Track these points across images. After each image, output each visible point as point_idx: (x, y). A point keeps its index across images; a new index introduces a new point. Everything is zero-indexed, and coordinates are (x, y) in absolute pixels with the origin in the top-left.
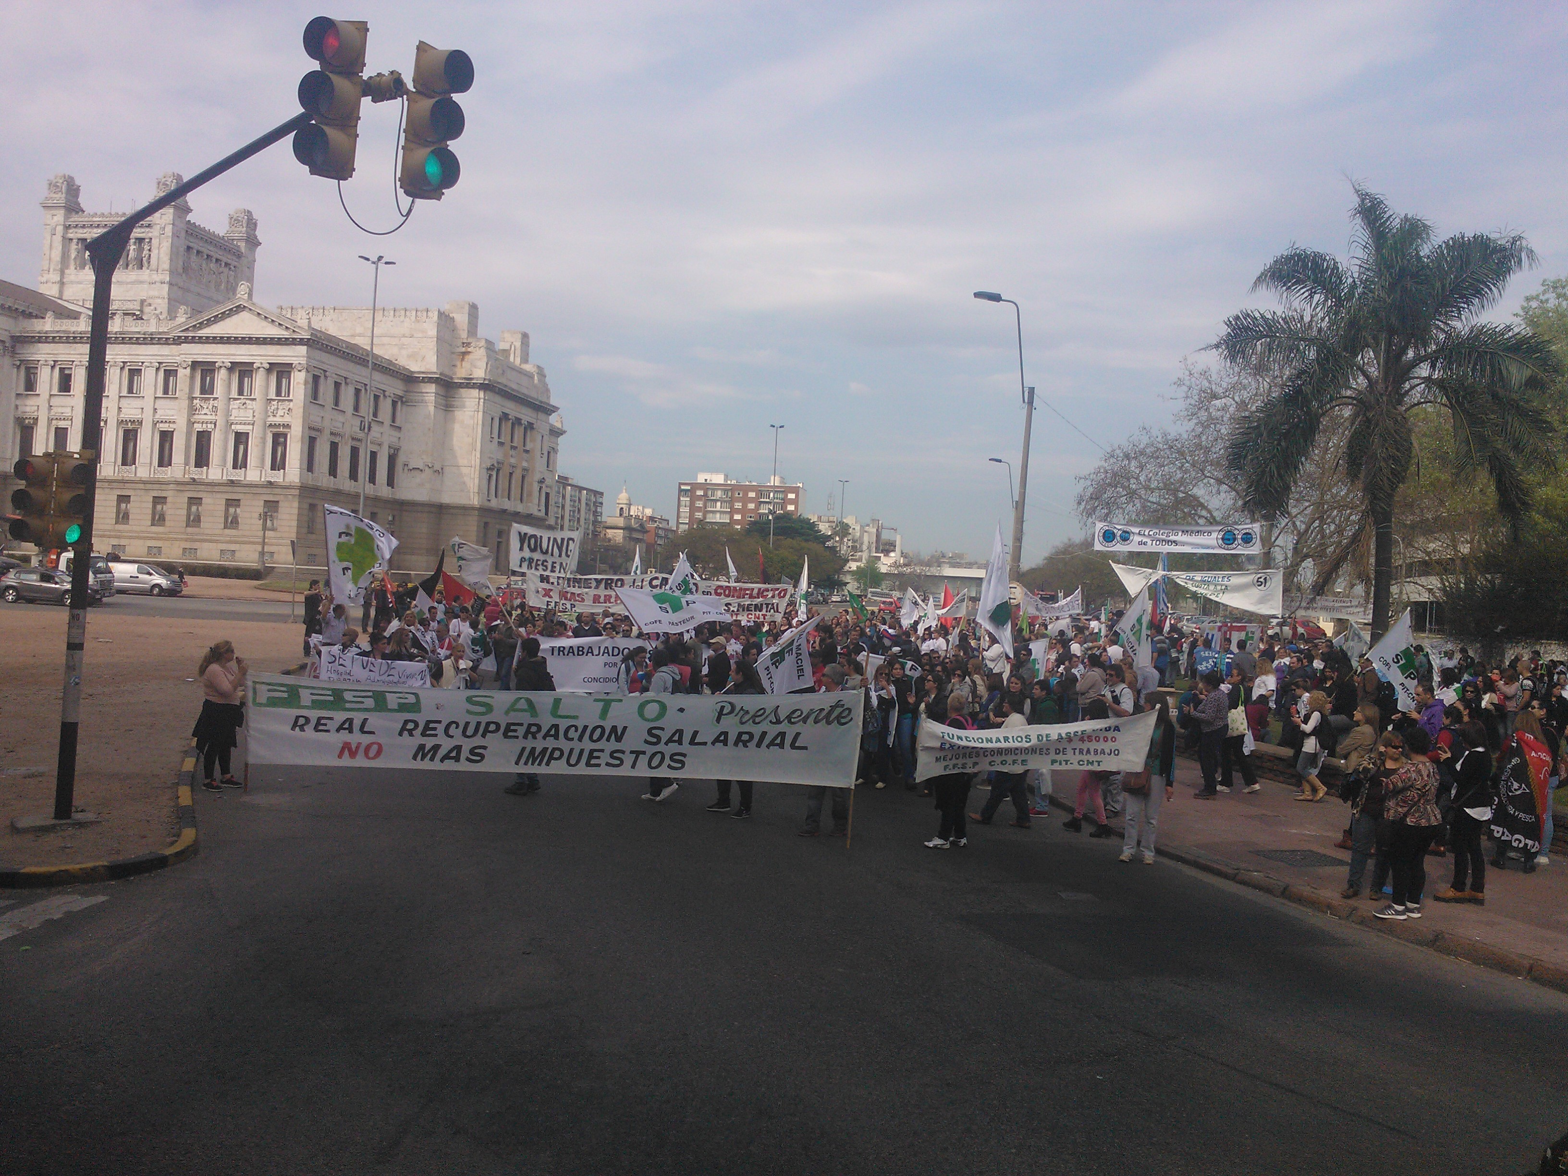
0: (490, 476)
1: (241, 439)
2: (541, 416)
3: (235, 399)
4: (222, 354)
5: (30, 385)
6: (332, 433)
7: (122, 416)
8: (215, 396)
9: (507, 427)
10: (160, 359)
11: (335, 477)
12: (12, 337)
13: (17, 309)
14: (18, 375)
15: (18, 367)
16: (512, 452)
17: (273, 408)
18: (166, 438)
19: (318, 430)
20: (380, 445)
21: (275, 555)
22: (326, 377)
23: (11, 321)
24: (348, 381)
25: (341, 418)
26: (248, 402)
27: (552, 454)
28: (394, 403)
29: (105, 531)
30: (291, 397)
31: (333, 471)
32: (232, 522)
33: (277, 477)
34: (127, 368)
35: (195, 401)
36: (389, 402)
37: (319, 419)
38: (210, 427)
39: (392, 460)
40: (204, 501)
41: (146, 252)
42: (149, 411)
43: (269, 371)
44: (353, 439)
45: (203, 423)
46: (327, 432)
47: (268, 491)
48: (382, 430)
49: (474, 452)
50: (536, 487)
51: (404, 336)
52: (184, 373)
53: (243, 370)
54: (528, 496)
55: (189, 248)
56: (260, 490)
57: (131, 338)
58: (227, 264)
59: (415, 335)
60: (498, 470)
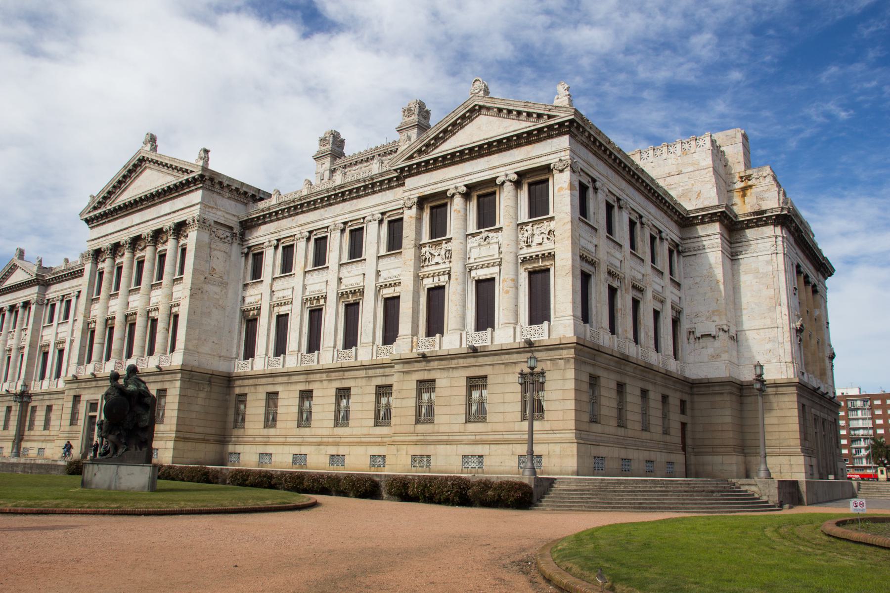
1: (485, 290)
3: (473, 235)
5: (257, 273)
8: (448, 236)
10: (383, 209)
12: (241, 222)
17: (526, 235)
18: (391, 305)
22: (596, 189)
23: (240, 206)
24: (622, 203)
26: (491, 235)
29: (322, 436)
30: (551, 214)
32: (476, 413)
33: (540, 334)
35: (423, 250)
36: (666, 246)
39: (676, 322)
43: (518, 184)
45: (433, 276)
46: (603, 268)
49: (778, 308)
51: (670, 175)
52: (409, 215)
53: (483, 195)
59: (684, 171)
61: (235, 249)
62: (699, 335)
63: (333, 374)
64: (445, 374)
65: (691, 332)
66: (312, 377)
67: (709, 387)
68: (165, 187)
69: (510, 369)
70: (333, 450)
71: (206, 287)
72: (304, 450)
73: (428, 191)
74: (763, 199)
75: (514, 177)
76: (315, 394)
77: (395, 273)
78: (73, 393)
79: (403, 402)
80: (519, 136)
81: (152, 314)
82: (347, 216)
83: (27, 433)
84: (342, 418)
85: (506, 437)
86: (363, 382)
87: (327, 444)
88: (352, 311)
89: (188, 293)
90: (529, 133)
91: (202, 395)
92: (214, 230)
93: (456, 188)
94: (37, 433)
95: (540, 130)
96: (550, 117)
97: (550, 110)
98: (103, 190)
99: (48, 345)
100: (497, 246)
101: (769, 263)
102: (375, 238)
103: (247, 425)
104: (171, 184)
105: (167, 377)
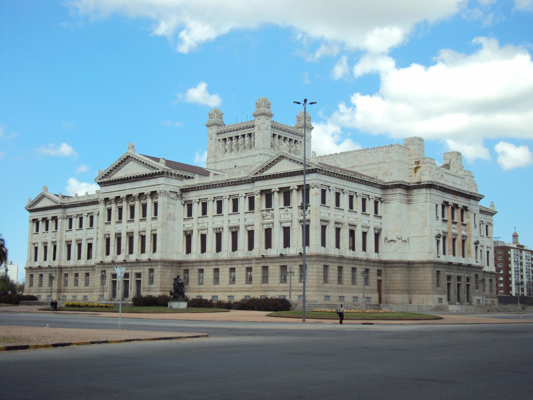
0: (438, 242)
1: (287, 231)
2: (472, 202)
3: (282, 209)
4: (274, 185)
6: (336, 223)
7: (230, 225)
9: (448, 211)
11: (325, 247)
12: (180, 190)
13: (182, 175)
14: (184, 209)
15: (184, 205)
16: (454, 226)
18: (251, 234)
19: (327, 221)
20: (368, 228)
25: (341, 213)
26: (288, 209)
27: (489, 227)
28: (376, 203)
31: (353, 248)
34: (231, 199)
37: (327, 215)
38: (271, 225)
39: (377, 236)
40: (269, 268)
41: (253, 140)
42: (242, 220)
43: (298, 190)
44: (350, 225)
48: (369, 219)
50: (473, 247)
52: (257, 198)
53: (286, 193)
54: (468, 253)
55: (274, 135)
56: (297, 260)
57: (232, 182)
58: (296, 141)
60: (444, 238)
61: (179, 203)
64: (272, 264)
65: (386, 239)
66: (219, 263)
68: (144, 174)
69: (295, 263)
70: (229, 294)
72: (216, 294)
73: (264, 188)
74: (423, 175)
75: (297, 188)
76: (220, 270)
77: (252, 220)
78: (101, 269)
79: (257, 273)
81: (141, 233)
83: (63, 288)
84: (233, 280)
86: (240, 266)
87: (226, 291)
88: (235, 236)
89: (160, 226)
91: (169, 271)
94: (70, 288)
96: (309, 166)
98: (107, 169)
99: (71, 241)
101: (423, 206)
102: (244, 204)
103: (189, 283)
104: (148, 173)
105: (154, 264)
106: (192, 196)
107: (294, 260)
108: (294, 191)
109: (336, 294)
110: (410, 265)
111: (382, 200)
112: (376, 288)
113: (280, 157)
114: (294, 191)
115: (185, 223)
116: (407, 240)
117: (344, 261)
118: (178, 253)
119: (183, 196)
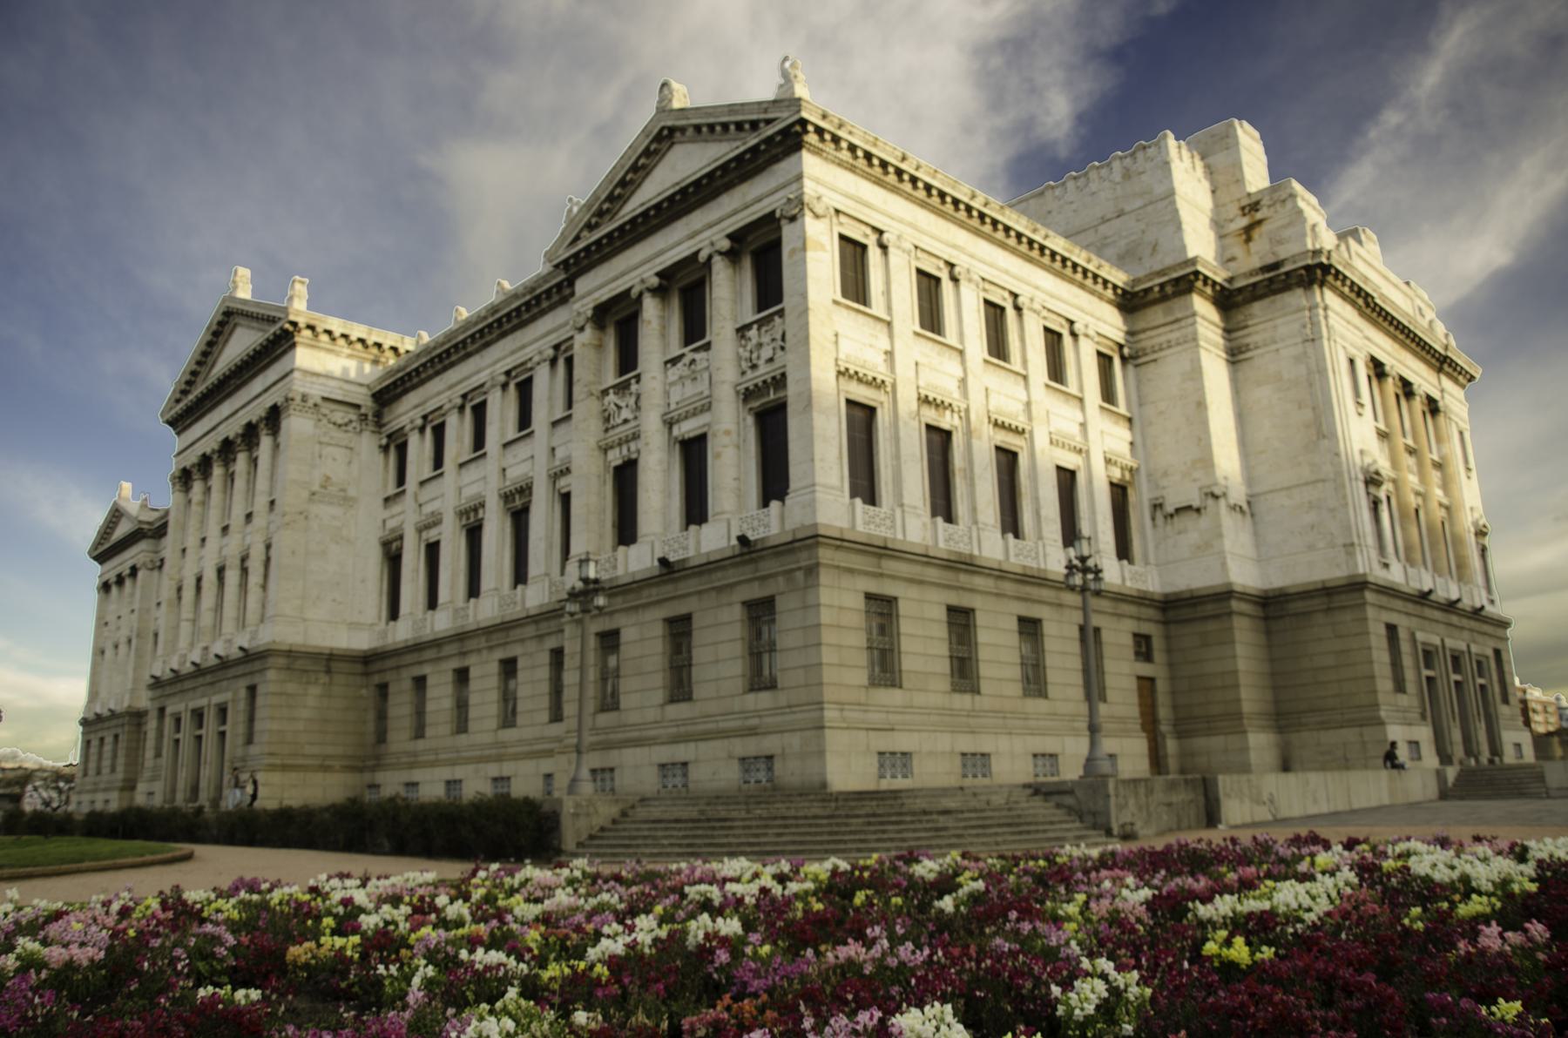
6: (925, 401)
15: (385, 449)
20: (1080, 451)
21: (777, 765)
26: (698, 356)
34: (512, 386)
35: (607, 399)
36: (1088, 351)
43: (732, 255)
47: (746, 572)
51: (1104, 221)
56: (732, 576)
61: (368, 444)
62: (1170, 509)
63: (495, 636)
65: (1157, 506)
67: (1195, 605)
71: (316, 509)
75: (725, 244)
80: (724, 168)
82: (509, 360)
85: (722, 725)
86: (531, 646)
90: (739, 159)
92: (324, 411)
93: (643, 281)
95: (754, 150)
96: (768, 122)
97: (766, 111)
100: (706, 375)
106: (407, 412)
107: (719, 579)
108: (719, 265)
109: (944, 742)
110: (1273, 607)
111: (1126, 351)
112: (1134, 711)
113: (659, 138)
114: (719, 265)
115: (387, 514)
116: (1245, 507)
117: (979, 582)
118: (354, 626)
119: (385, 420)
